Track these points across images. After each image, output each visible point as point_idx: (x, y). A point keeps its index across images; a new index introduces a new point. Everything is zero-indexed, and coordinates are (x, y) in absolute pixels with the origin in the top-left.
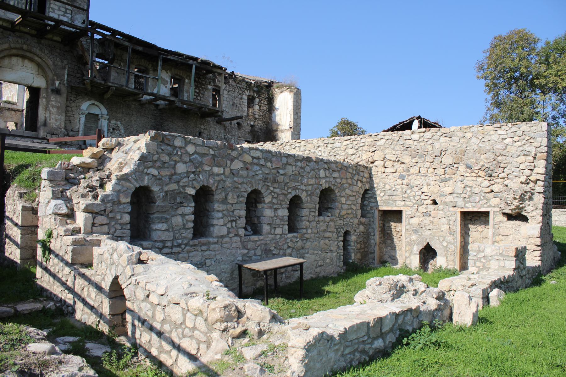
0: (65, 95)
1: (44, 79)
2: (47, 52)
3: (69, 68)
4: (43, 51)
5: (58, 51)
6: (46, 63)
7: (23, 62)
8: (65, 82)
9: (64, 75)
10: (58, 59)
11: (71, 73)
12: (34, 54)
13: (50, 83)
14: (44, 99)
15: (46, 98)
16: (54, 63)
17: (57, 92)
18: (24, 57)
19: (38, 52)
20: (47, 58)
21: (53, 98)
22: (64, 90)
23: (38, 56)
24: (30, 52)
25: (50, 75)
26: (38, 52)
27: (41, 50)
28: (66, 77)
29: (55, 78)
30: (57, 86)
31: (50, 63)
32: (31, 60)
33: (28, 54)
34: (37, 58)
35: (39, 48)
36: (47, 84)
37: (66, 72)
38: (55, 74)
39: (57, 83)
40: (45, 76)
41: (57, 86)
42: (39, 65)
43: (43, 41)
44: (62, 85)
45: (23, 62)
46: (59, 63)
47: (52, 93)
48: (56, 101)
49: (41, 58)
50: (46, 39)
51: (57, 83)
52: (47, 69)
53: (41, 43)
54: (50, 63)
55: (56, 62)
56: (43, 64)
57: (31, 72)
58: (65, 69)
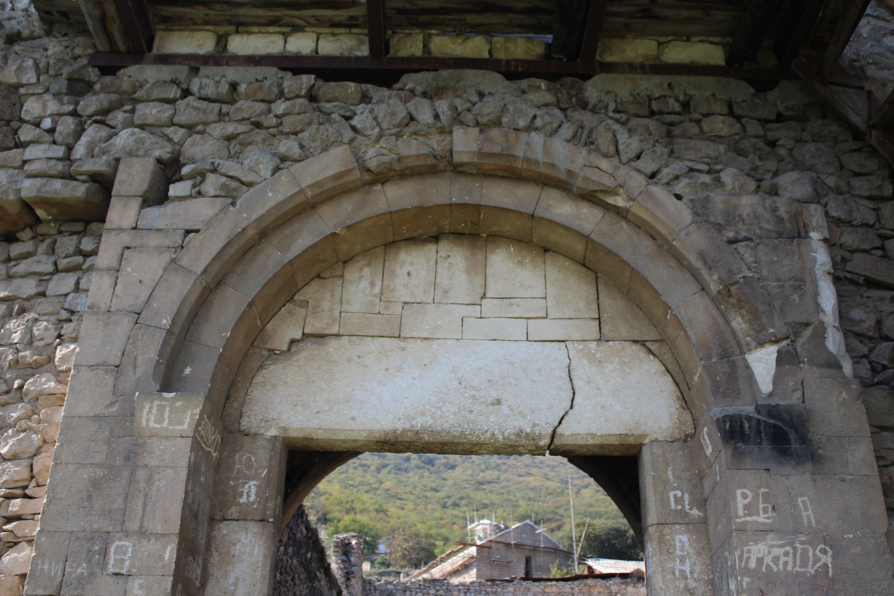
0: (860, 456)
1: (652, 366)
2: (629, 144)
3: (835, 222)
4: (604, 141)
5: (720, 125)
6: (639, 225)
7: (480, 270)
8: (834, 342)
9: (802, 283)
10: (727, 176)
11: (861, 265)
12: (546, 181)
13: (701, 374)
14: (682, 540)
15: (701, 528)
16: (700, 210)
17: (777, 436)
18: (473, 230)
19: (560, 152)
20: (637, 181)
21: (749, 496)
22: (836, 409)
23: (562, 185)
24: (513, 175)
25: (694, 311)
26: (560, 152)
27: (584, 139)
28: (828, 297)
29: (739, 323)
30: (765, 384)
31: (671, 211)
32: (534, 240)
33: (498, 194)
34: (562, 209)
35: (567, 131)
36: (685, 401)
37: (822, 258)
38: (731, 295)
39: (763, 363)
40: (658, 337)
41: (765, 384)
42: (594, 264)
43: (592, 90)
44: (809, 373)
45: (480, 270)
46: (748, 203)
47: (738, 455)
48: (787, 529)
49: (591, 197)
50: (609, 68)
51: (763, 363)
52: (659, 273)
53: (584, 105)
54: (671, 211)
55: (718, 200)
56: (621, 239)
57: (540, 329)
58: (799, 234)
